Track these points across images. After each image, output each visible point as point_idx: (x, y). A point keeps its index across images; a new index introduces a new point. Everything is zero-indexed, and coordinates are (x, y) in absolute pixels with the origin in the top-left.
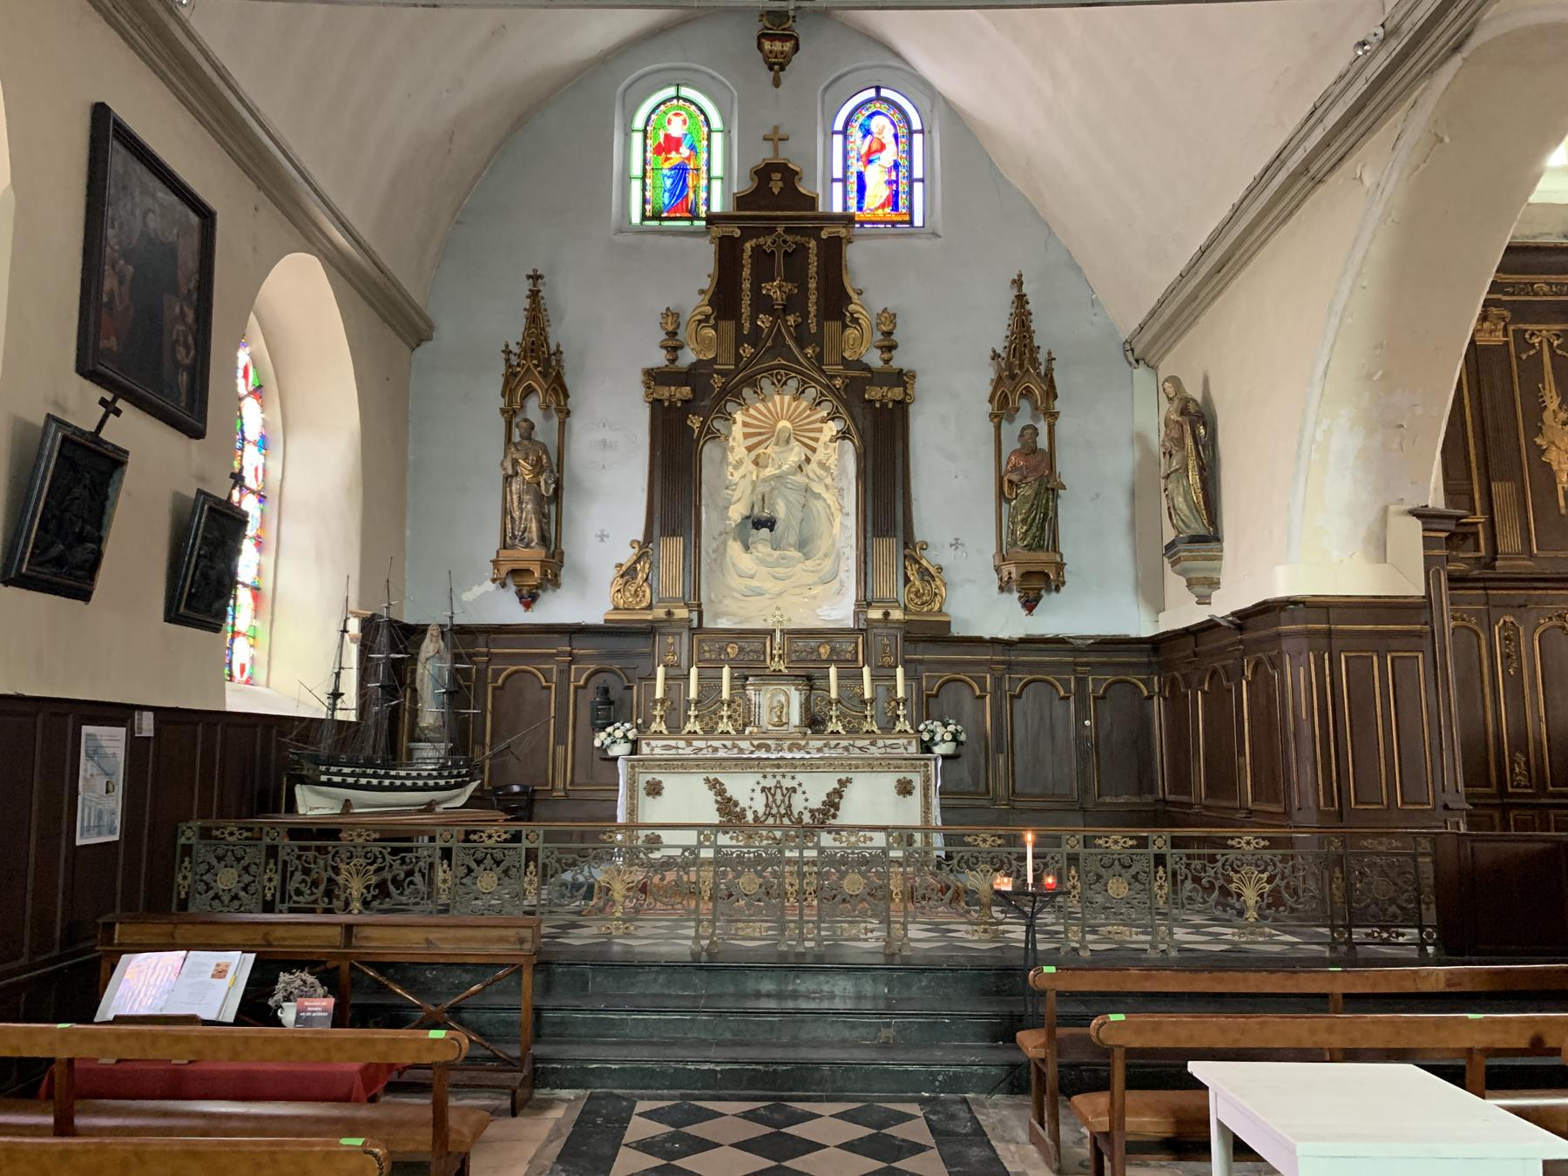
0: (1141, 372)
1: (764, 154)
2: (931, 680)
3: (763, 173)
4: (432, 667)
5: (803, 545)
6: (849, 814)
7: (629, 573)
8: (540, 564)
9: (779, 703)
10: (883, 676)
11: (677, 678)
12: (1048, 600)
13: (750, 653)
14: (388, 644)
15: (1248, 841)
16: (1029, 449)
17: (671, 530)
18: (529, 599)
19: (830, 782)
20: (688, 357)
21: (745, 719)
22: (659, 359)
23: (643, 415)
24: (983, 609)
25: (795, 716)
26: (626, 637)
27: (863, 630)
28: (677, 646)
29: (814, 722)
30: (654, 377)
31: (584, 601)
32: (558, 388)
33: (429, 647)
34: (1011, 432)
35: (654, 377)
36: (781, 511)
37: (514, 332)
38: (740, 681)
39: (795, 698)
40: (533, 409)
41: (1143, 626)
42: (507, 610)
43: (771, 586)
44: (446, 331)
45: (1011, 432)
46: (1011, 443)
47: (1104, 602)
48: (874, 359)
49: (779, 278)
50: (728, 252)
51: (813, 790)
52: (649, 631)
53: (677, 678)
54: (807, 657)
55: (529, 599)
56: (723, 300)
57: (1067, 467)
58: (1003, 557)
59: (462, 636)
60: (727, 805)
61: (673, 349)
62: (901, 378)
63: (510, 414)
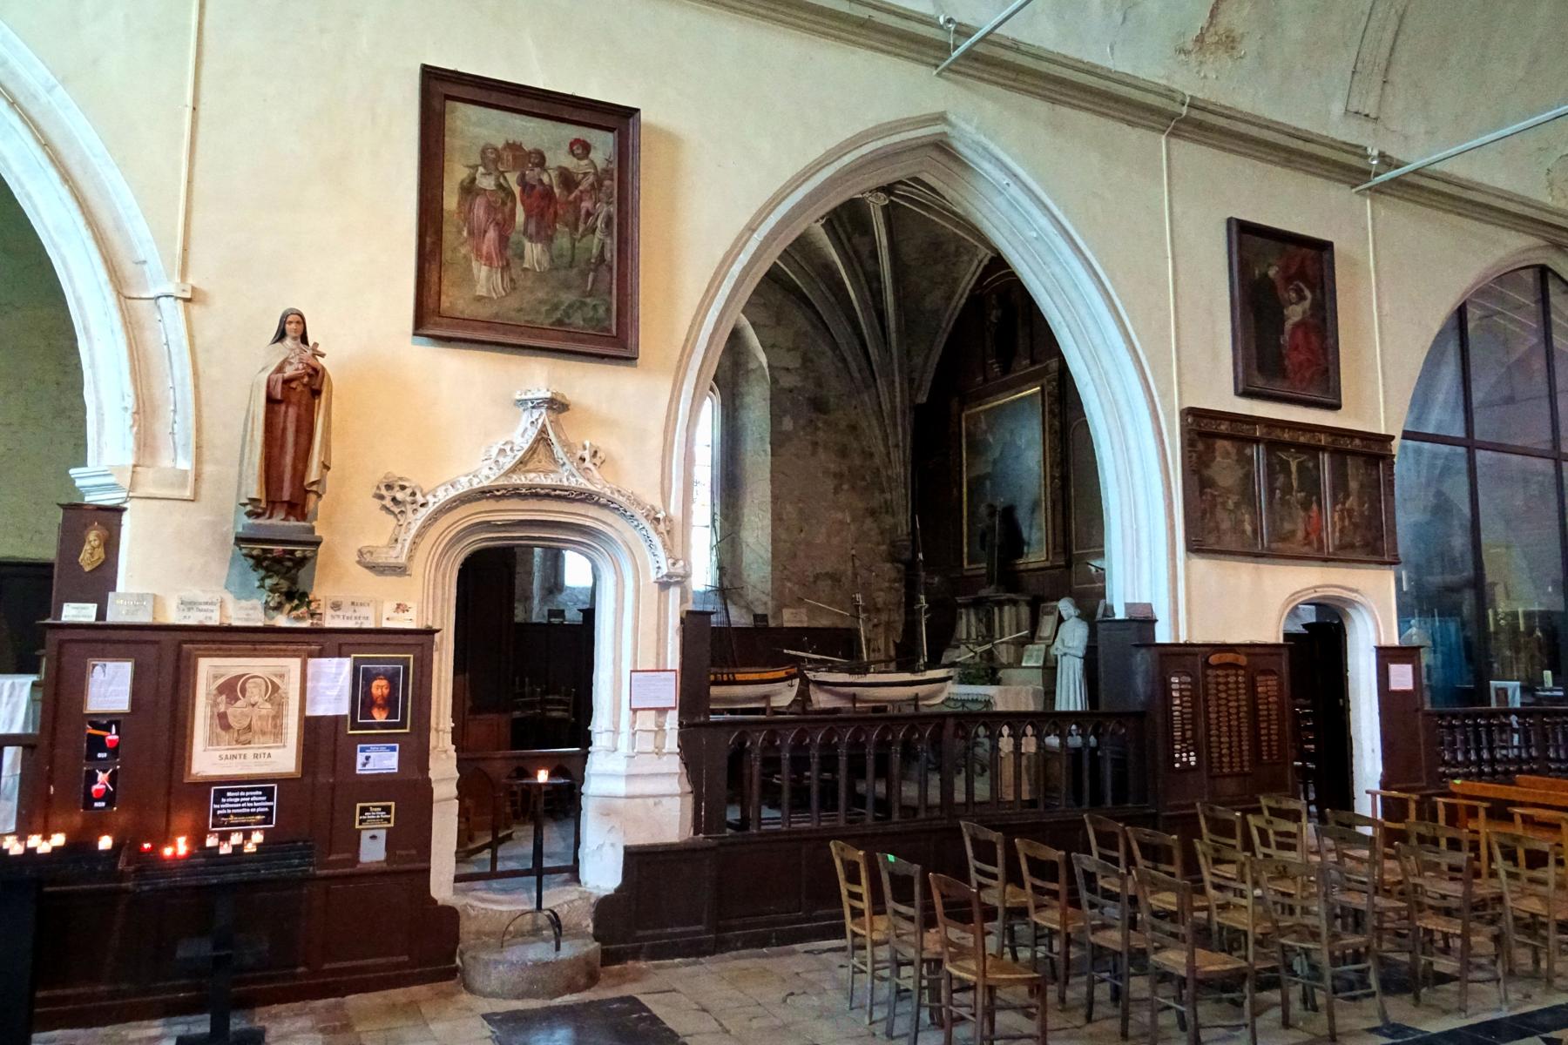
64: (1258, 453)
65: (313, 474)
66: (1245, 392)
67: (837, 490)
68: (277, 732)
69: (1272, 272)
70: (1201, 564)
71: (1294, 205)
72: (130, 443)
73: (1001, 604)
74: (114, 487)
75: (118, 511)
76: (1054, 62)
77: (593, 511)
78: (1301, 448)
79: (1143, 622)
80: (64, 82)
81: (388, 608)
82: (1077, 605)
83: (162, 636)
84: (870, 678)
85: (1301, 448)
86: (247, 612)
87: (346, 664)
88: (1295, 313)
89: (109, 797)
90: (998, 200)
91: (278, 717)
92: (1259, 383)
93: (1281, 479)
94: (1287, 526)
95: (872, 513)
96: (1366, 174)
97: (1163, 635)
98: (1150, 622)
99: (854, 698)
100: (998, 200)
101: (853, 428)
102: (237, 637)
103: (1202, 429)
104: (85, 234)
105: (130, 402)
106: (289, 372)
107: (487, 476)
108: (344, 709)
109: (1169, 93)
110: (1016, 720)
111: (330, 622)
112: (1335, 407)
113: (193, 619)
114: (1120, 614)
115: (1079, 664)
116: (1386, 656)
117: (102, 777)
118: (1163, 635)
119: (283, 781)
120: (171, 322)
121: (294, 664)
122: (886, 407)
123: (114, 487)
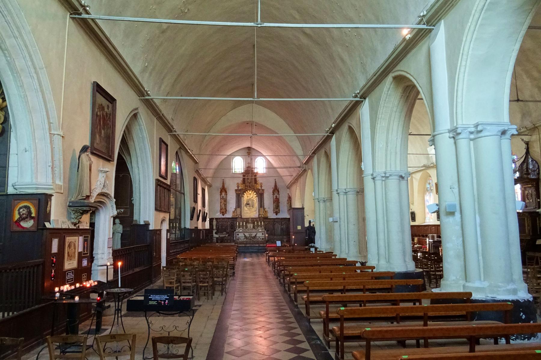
0: (288, 190)
1: (248, 165)
2: (266, 223)
3: (248, 167)
4: (215, 223)
5: (253, 206)
6: (257, 236)
7: (234, 212)
8: (224, 211)
9: (250, 226)
10: (261, 223)
11: (239, 224)
12: (278, 214)
13: (247, 220)
14: (211, 220)
15: (285, 237)
16: (276, 198)
17: (239, 207)
18: (223, 215)
19: (255, 234)
20: (240, 188)
21: (246, 227)
22: (237, 188)
23: (235, 195)
24: (271, 215)
25: (252, 227)
26: (234, 219)
27: (259, 218)
28: (239, 220)
29: (254, 227)
30: (236, 190)
31: (229, 215)
32: (226, 192)
33: (214, 220)
34: (275, 196)
35: (236, 190)
36: (250, 202)
37: (221, 186)
38: (246, 223)
39: (252, 225)
40: (223, 194)
41: (288, 217)
42: (221, 216)
43: (249, 212)
44: (213, 186)
45: (275, 196)
46: (275, 197)
47: (284, 214)
48: (260, 188)
49: (249, 179)
50: (244, 176)
51: (254, 235)
52: (236, 218)
53: (239, 224)
54: (253, 220)
55: (223, 215)
56: (244, 181)
57: (281, 200)
58: (274, 210)
59: (216, 219)
60: (245, 236)
61: (238, 187)
62: (263, 190)
63: (221, 194)
68: (75, 257)
72: (50, 176)
74: (52, 189)
75: (51, 195)
77: (106, 199)
79: (147, 225)
80: (46, 68)
82: (120, 221)
83: (61, 231)
86: (67, 225)
89: (54, 276)
90: (138, 127)
91: (75, 253)
96: (171, 131)
97: (151, 227)
98: (149, 224)
100: (138, 127)
102: (69, 231)
104: (45, 113)
105: (50, 164)
107: (98, 191)
111: (80, 228)
113: (64, 226)
114: (142, 223)
115: (120, 235)
117: (53, 271)
118: (151, 227)
119: (74, 269)
120: (58, 141)
121: (77, 238)
123: (52, 189)
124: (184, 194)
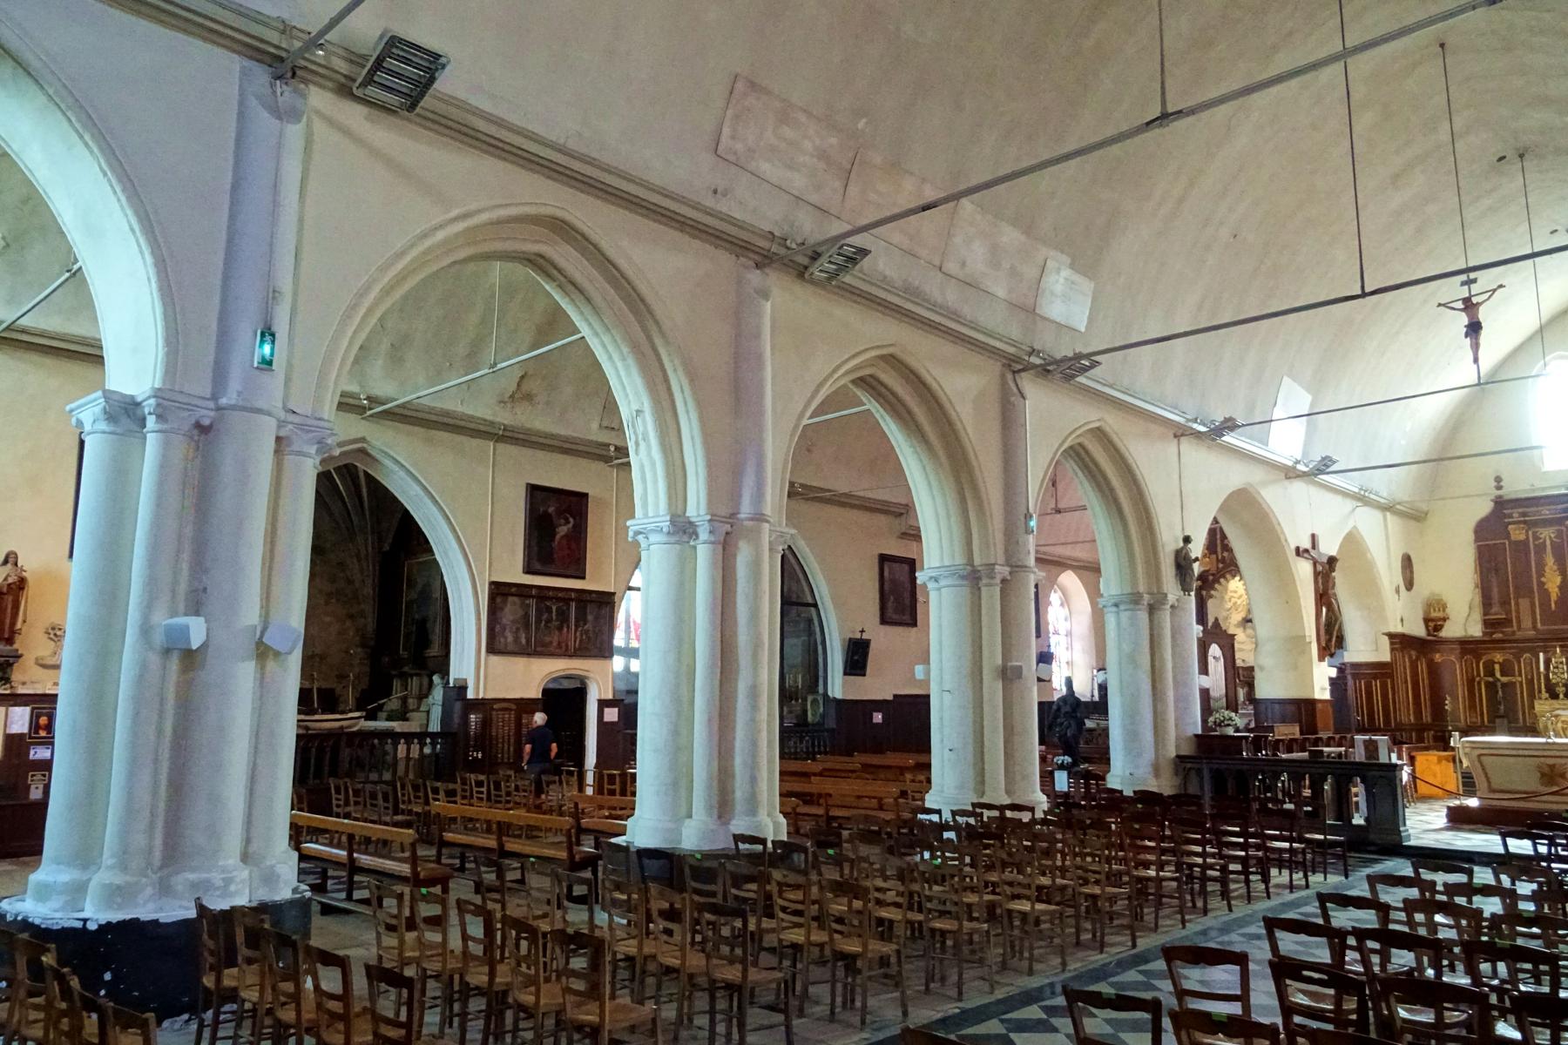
64: (532, 602)
65: (19, 625)
66: (528, 570)
67: (327, 603)
69: (551, 510)
70: (494, 659)
71: (562, 475)
73: (412, 676)
76: (631, 180)
78: (559, 599)
79: (462, 689)
81: (49, 685)
84: (317, 717)
85: (559, 599)
87: (28, 709)
88: (563, 530)
92: (538, 566)
93: (545, 616)
94: (547, 639)
95: (351, 617)
97: (470, 695)
99: (307, 728)
101: (341, 564)
103: (500, 592)
106: (10, 580)
108: (26, 730)
109: (492, 423)
110: (409, 737)
111: (21, 690)
112: (583, 578)
116: (603, 704)
118: (470, 695)
122: (363, 552)
124: (815, 605)
